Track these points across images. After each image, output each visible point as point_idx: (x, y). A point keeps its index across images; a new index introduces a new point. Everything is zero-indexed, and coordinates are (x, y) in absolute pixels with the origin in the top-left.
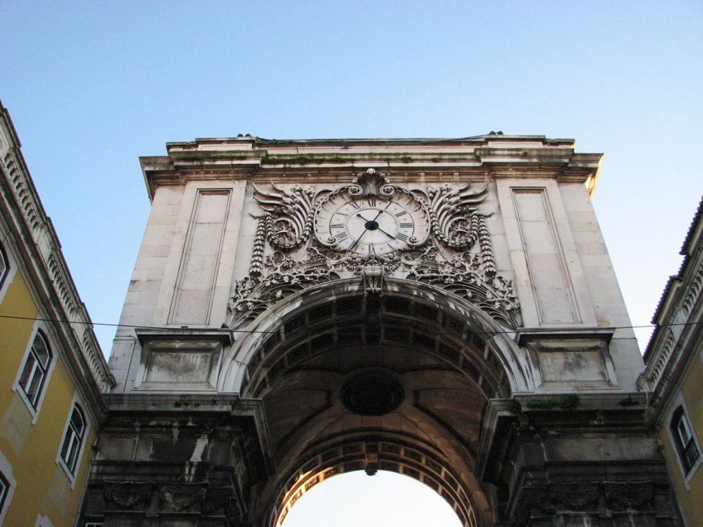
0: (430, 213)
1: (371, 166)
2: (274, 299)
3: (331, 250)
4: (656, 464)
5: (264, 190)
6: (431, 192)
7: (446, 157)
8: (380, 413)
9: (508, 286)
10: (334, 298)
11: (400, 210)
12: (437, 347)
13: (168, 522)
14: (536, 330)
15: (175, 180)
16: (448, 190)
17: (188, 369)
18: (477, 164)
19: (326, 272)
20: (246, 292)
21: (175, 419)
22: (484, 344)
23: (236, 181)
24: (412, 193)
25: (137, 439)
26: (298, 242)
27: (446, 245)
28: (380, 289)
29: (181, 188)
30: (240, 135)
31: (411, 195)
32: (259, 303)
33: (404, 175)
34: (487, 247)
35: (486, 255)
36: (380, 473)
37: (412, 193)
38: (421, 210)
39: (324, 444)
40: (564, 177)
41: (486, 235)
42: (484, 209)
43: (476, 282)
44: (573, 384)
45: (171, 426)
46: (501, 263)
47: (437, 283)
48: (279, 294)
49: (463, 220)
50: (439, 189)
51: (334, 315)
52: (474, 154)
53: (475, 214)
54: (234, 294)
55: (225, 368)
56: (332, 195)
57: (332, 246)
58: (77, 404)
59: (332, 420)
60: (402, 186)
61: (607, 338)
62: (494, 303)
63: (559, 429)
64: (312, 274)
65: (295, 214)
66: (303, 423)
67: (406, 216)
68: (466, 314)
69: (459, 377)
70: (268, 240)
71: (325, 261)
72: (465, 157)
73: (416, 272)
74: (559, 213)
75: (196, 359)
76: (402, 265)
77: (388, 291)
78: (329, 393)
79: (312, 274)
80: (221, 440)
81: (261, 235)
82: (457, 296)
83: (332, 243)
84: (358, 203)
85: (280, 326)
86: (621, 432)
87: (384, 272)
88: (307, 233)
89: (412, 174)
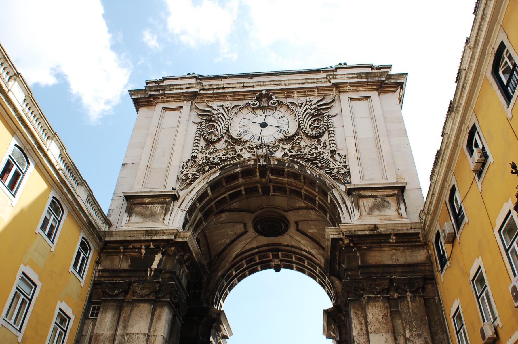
0: (299, 116)
1: (264, 89)
2: (204, 172)
3: (238, 141)
4: (427, 266)
5: (202, 106)
6: (300, 103)
8: (276, 236)
9: (343, 159)
10: (239, 170)
11: (281, 115)
12: (303, 196)
13: (136, 304)
15: (150, 103)
16: (310, 101)
18: (329, 84)
19: (235, 154)
20: (188, 168)
21: (143, 244)
22: (328, 194)
23: (185, 102)
24: (288, 104)
25: (122, 256)
26: (219, 137)
27: (307, 135)
28: (266, 163)
29: (153, 107)
30: (189, 74)
31: (288, 105)
32: (195, 174)
33: (284, 93)
34: (332, 135)
35: (331, 140)
36: (283, 270)
37: (288, 104)
38: (293, 114)
39: (246, 254)
40: (383, 89)
41: (332, 127)
43: (323, 157)
44: (378, 217)
45: (140, 248)
46: (340, 145)
47: (300, 158)
48: (207, 168)
49: (319, 119)
51: (241, 179)
53: (326, 115)
54: (181, 170)
56: (241, 108)
57: (239, 139)
58: (83, 238)
59: (250, 240)
60: (283, 100)
61: (402, 189)
62: (334, 169)
63: (368, 245)
64: (227, 156)
65: (218, 120)
66: (232, 242)
67: (285, 118)
68: (316, 176)
69: (318, 213)
70: (203, 137)
71: (234, 148)
72: (321, 80)
73: (288, 153)
74: (378, 111)
75: (158, 208)
76: (280, 148)
77: (271, 164)
78: (245, 225)
79: (227, 156)
80: (169, 255)
81: (199, 134)
82: (311, 166)
83: (239, 137)
84: (256, 112)
85: (207, 187)
86: (407, 246)
87: (269, 152)
88: (225, 131)
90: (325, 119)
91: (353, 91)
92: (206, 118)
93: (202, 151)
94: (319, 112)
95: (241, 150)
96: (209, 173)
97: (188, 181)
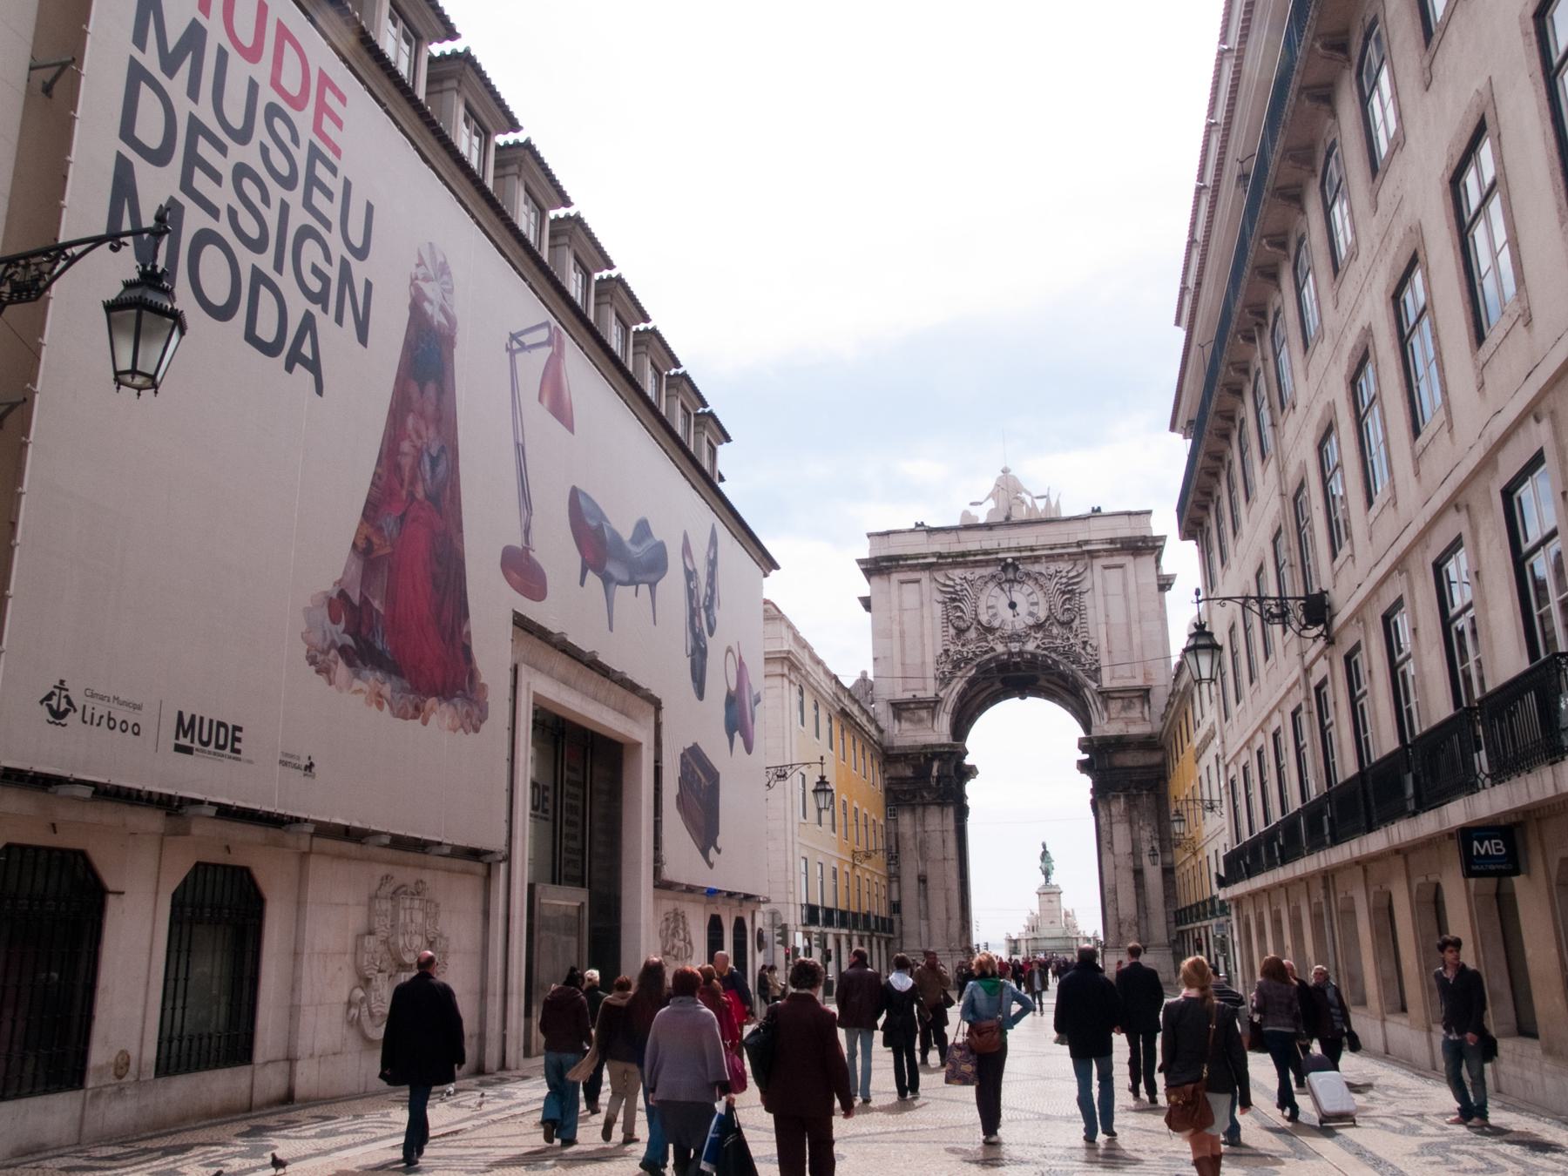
1: (1009, 556)
2: (960, 669)
3: (990, 630)
5: (940, 577)
10: (993, 665)
17: (921, 720)
18: (1080, 550)
30: (917, 525)
42: (1086, 585)
45: (919, 758)
48: (962, 665)
52: (1078, 542)
62: (1084, 665)
74: (1132, 588)
75: (924, 714)
89: (1037, 559)
94: (1070, 588)
96: (964, 670)
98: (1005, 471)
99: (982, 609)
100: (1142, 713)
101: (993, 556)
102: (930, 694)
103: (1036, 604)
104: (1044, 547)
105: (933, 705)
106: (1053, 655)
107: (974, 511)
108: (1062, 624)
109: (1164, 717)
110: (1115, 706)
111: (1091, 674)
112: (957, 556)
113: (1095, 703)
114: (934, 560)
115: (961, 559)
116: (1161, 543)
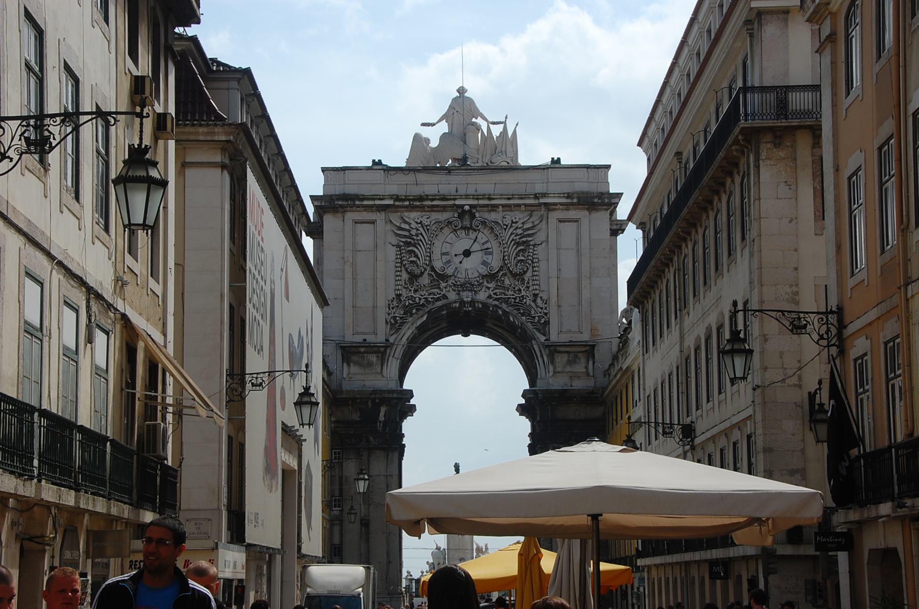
0: (503, 244)
3: (444, 277)
5: (395, 218)
6: (505, 225)
7: (517, 196)
11: (485, 239)
14: (554, 342)
17: (370, 365)
18: (537, 202)
19: (440, 294)
27: (511, 272)
29: (340, 215)
30: (374, 161)
32: (403, 317)
34: (536, 273)
42: (540, 237)
48: (414, 311)
50: (510, 222)
55: (389, 363)
62: (535, 317)
71: (439, 284)
73: (492, 294)
74: (585, 243)
75: (373, 358)
89: (494, 208)
90: (531, 251)
91: (563, 210)
92: (404, 240)
93: (406, 286)
94: (524, 239)
95: (445, 288)
97: (397, 325)
98: (461, 91)
99: (436, 255)
100: (586, 368)
101: (451, 202)
102: (381, 338)
103: (491, 253)
104: (501, 197)
105: (382, 351)
106: (504, 306)
107: (426, 132)
108: (514, 275)
109: (607, 373)
110: (561, 359)
111: (541, 327)
112: (413, 200)
113: (542, 356)
114: (391, 202)
115: (418, 202)
116: (613, 201)
